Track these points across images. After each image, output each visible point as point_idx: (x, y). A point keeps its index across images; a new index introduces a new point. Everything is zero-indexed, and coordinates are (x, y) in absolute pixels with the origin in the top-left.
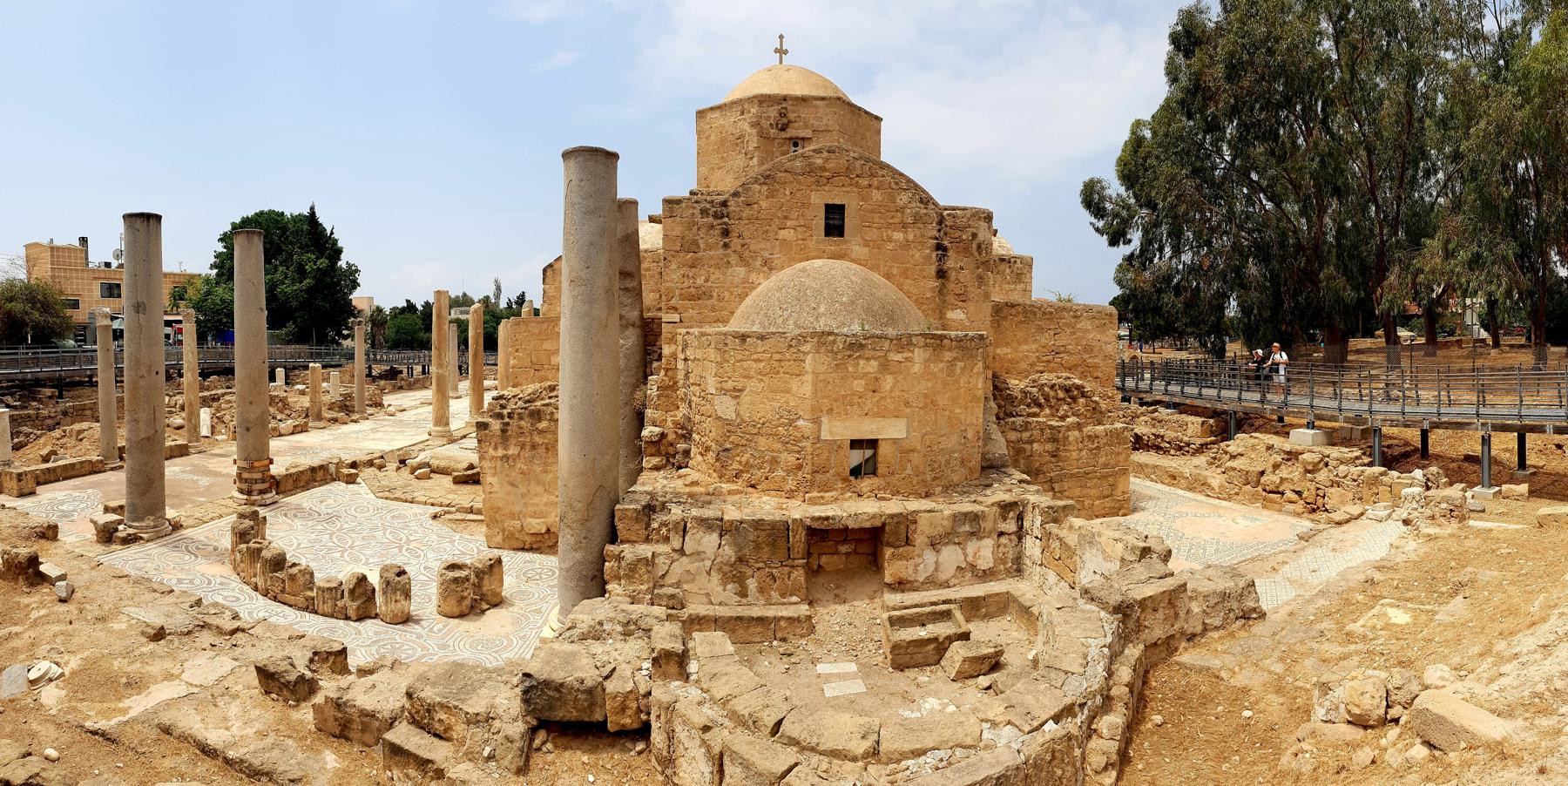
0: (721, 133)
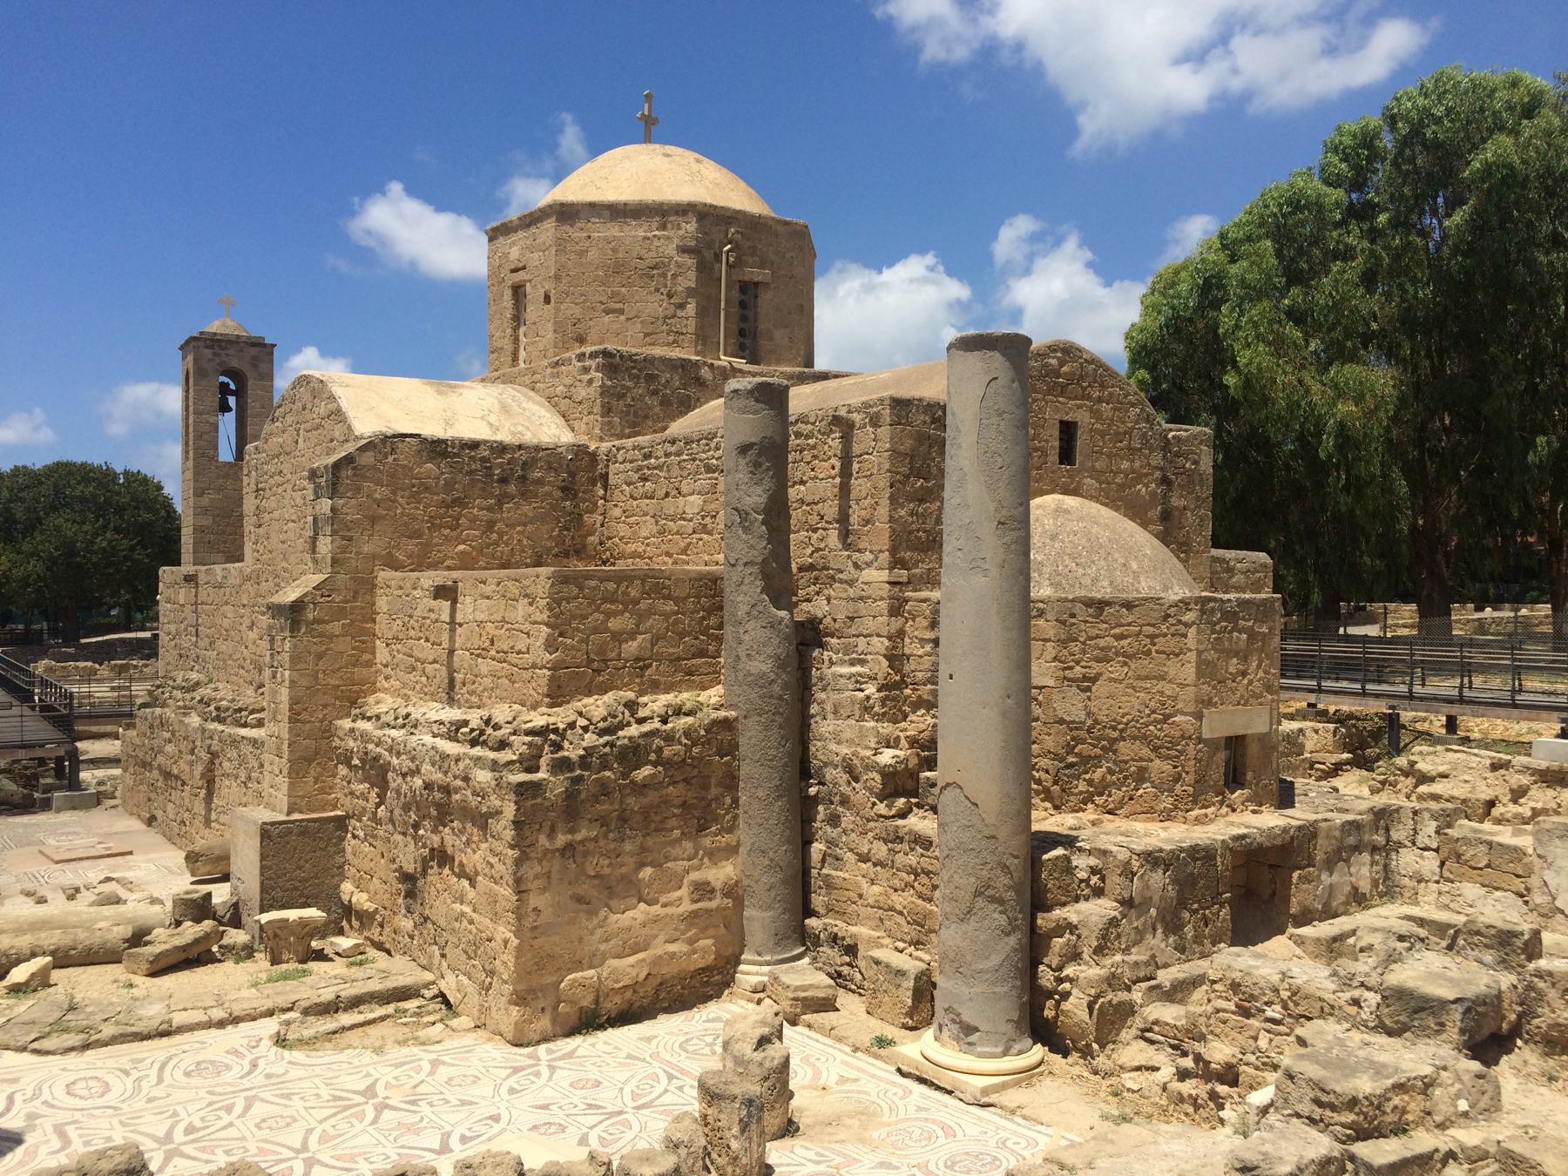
0: (614, 250)
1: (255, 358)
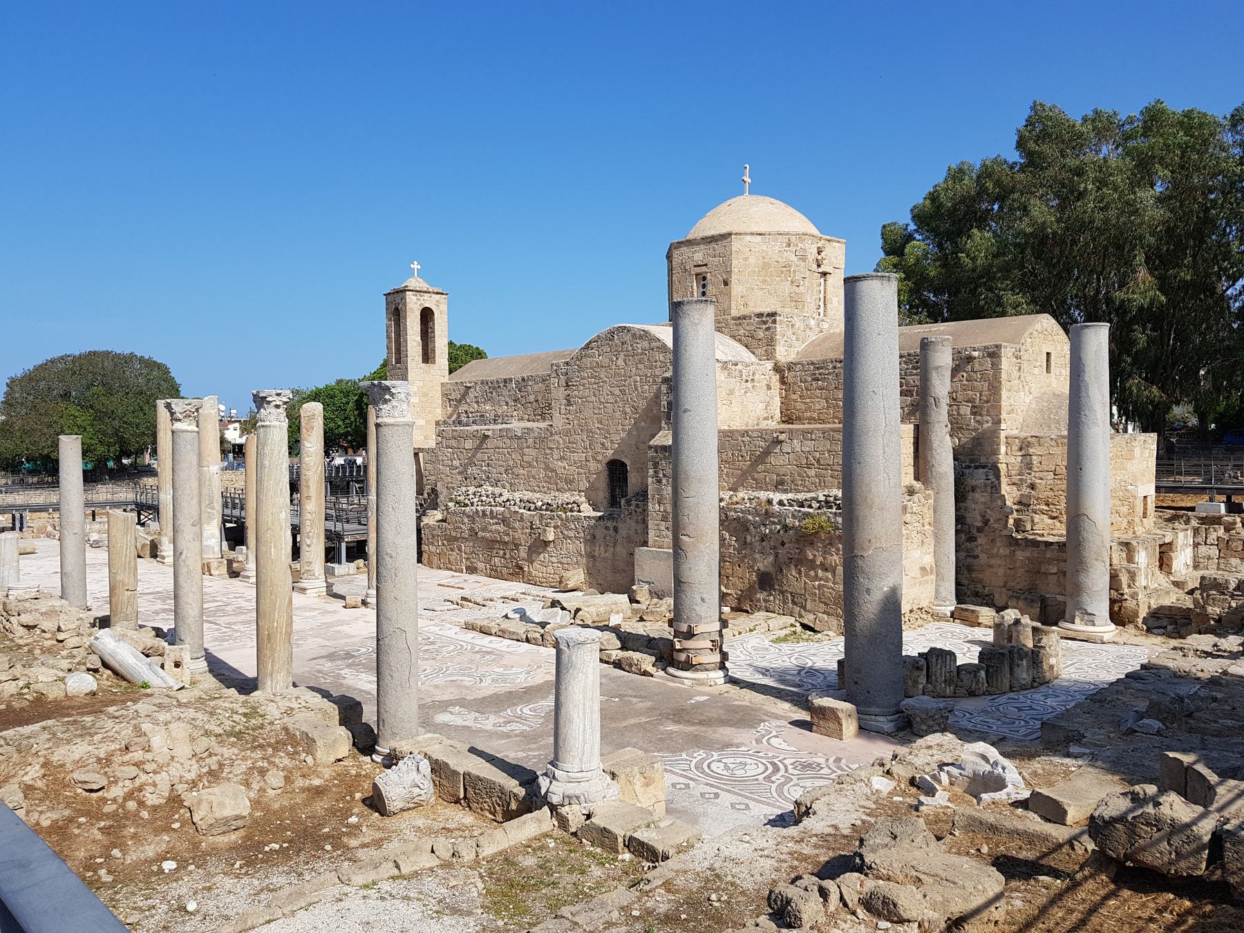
0: (763, 258)
1: (437, 301)
